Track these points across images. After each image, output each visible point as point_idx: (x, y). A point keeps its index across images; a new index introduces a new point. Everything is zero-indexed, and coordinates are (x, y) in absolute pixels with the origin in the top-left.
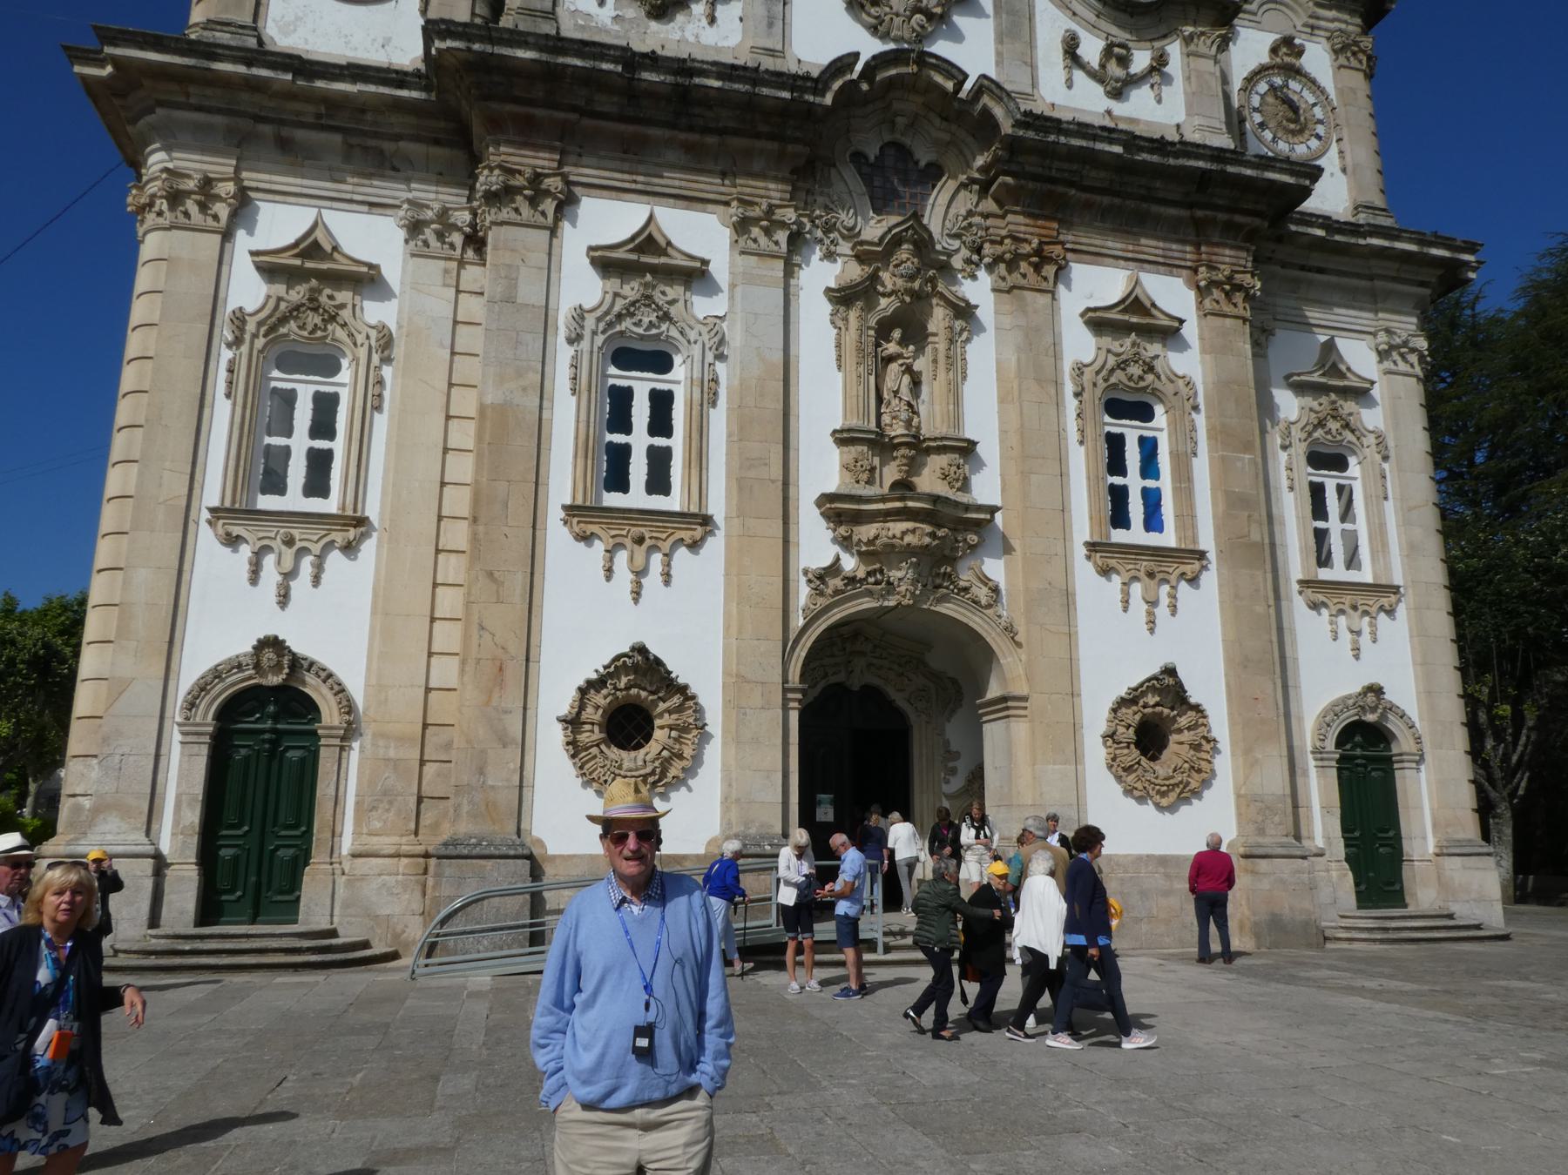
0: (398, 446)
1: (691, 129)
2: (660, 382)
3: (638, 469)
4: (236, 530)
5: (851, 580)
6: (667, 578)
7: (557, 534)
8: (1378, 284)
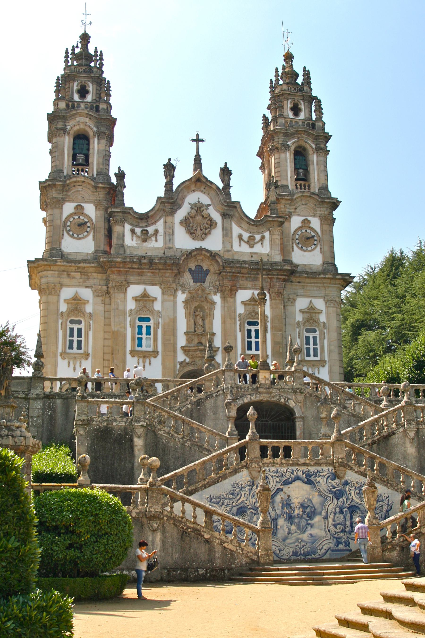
0: (94, 339)
1: (153, 269)
2: (148, 324)
5: (188, 363)
6: (150, 364)
7: (128, 356)
8: (325, 285)
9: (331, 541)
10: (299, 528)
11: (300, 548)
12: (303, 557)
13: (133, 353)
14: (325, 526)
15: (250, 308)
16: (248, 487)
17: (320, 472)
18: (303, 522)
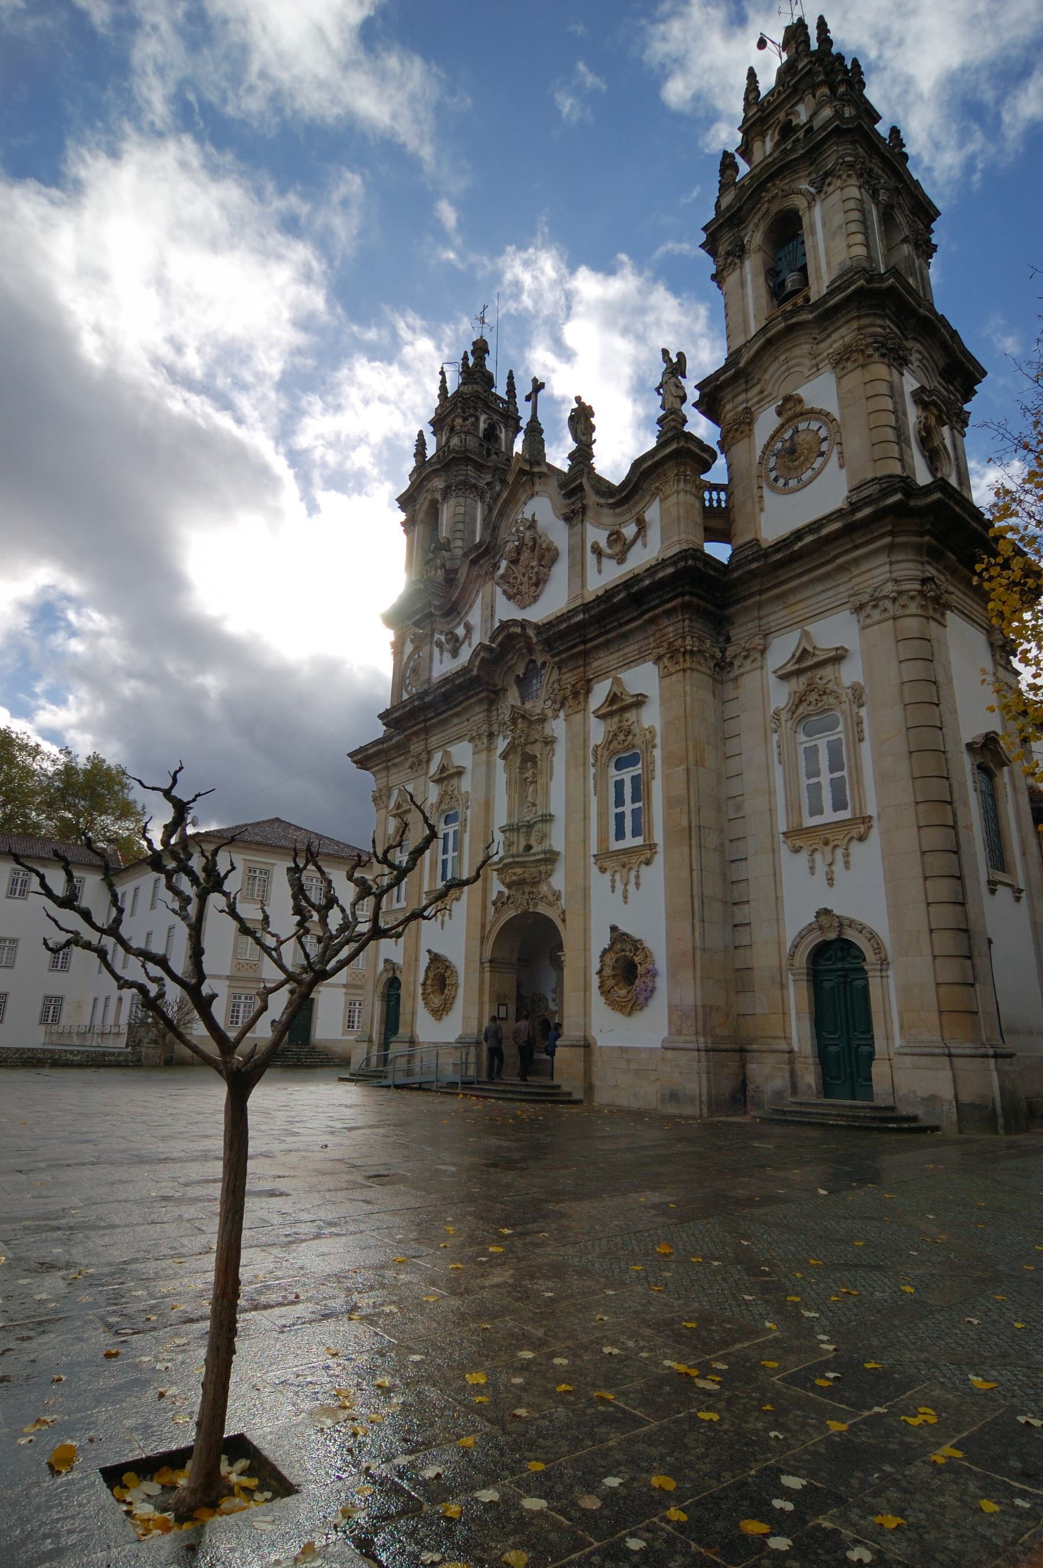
4: (798, 843)
15: (614, 723)
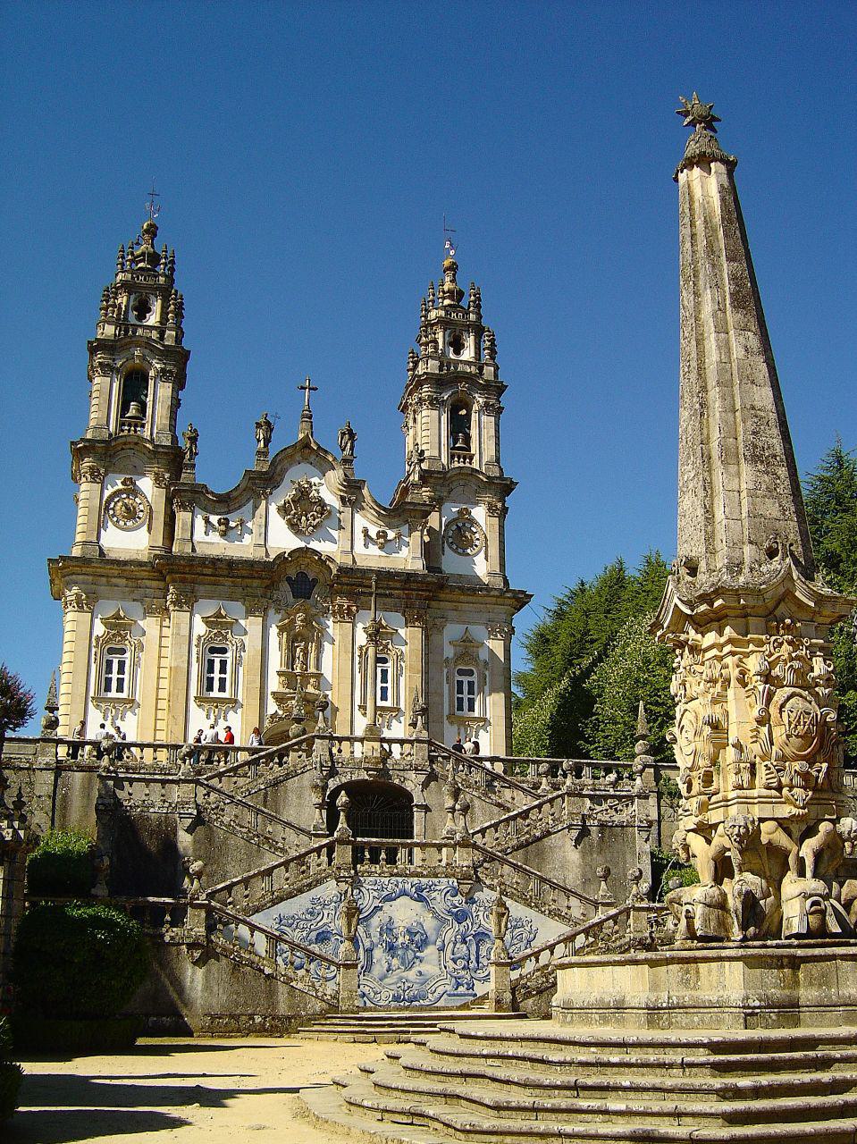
3: (216, 684)
7: (193, 705)
9: (447, 981)
10: (403, 964)
11: (404, 991)
12: (407, 1004)
13: (201, 700)
14: (440, 961)
16: (333, 904)
17: (436, 885)
18: (410, 955)
